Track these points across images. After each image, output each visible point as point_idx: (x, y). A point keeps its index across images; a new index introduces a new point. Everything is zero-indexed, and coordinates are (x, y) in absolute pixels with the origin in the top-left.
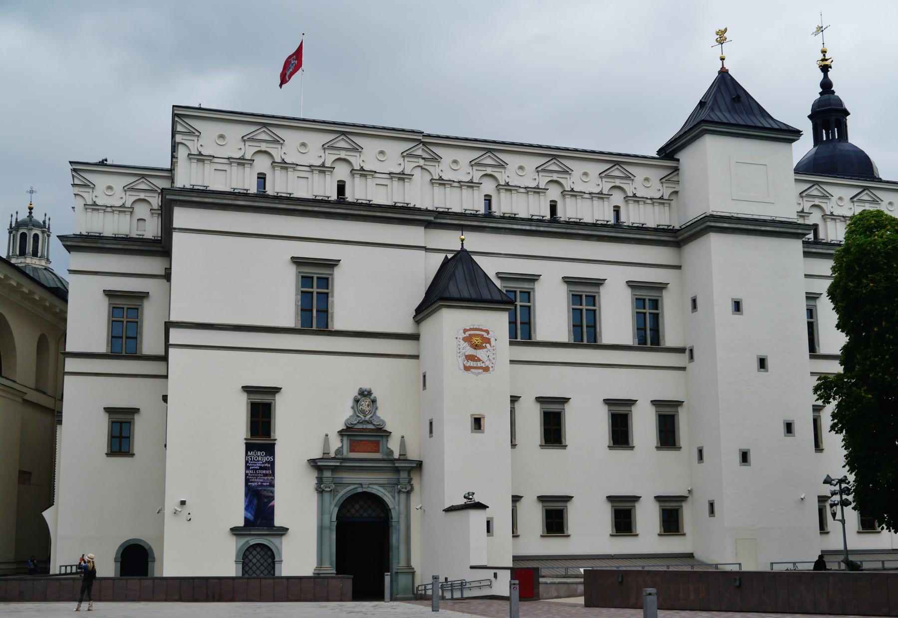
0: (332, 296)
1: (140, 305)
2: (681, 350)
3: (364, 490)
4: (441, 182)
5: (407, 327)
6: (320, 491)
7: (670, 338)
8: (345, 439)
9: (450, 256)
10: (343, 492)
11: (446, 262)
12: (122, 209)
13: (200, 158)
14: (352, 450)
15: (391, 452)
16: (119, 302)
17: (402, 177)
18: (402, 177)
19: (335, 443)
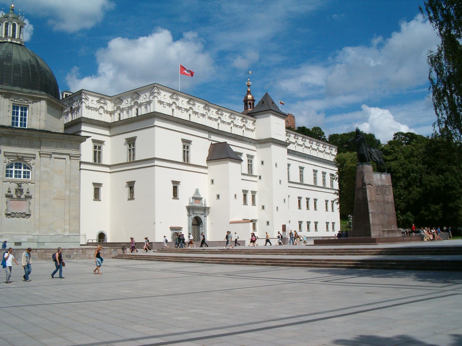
0: (190, 152)
1: (102, 146)
2: (256, 176)
3: (198, 216)
4: (210, 118)
5: (205, 164)
6: (189, 216)
7: (255, 173)
8: (194, 199)
9: (213, 143)
10: (193, 216)
11: (212, 144)
12: (96, 110)
13: (161, 102)
14: (195, 203)
15: (203, 203)
16: (96, 144)
17: (203, 115)
18: (203, 115)
19: (192, 201)
